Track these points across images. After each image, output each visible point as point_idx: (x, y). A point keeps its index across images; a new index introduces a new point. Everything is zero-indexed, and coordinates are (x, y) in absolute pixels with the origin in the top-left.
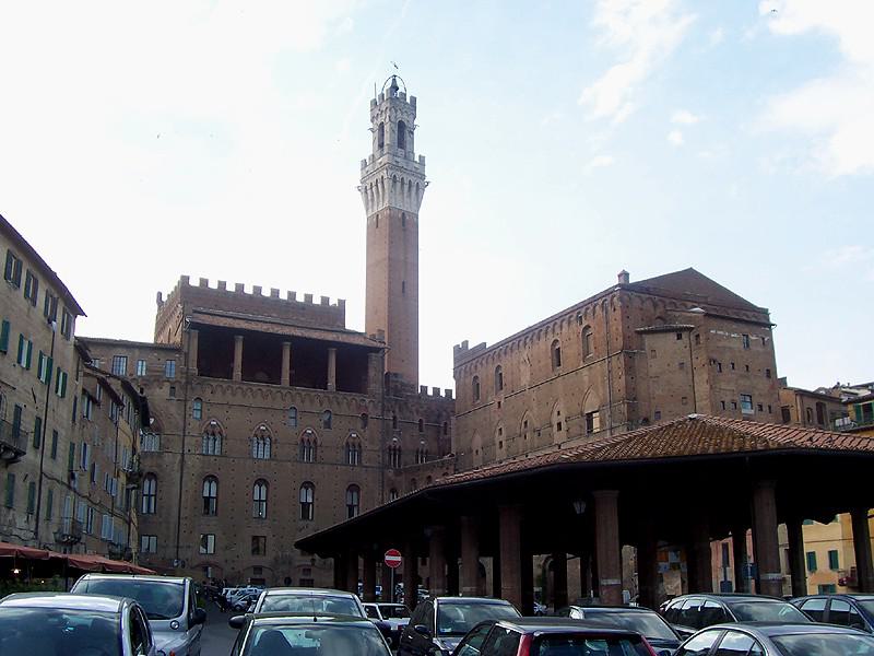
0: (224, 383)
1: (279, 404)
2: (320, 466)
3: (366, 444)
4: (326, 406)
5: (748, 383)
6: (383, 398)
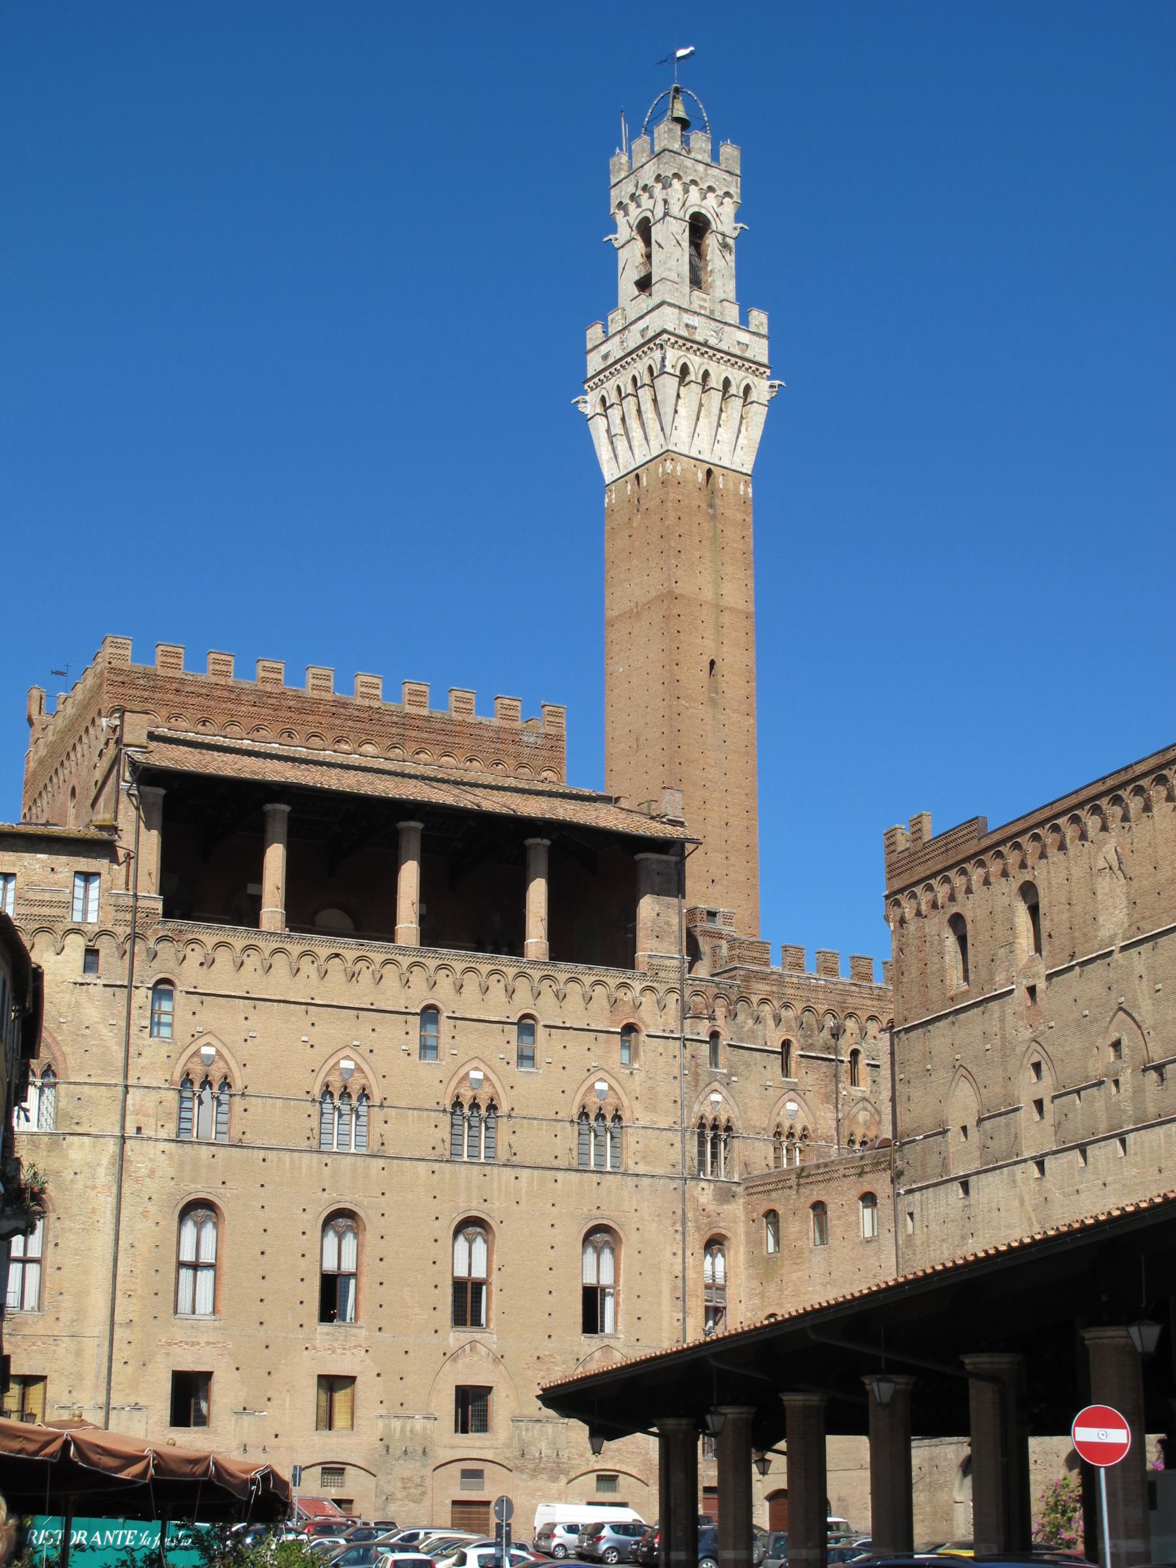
0: (238, 937)
1: (391, 994)
2: (509, 1173)
3: (634, 1112)
4: (523, 1003)
6: (682, 980)
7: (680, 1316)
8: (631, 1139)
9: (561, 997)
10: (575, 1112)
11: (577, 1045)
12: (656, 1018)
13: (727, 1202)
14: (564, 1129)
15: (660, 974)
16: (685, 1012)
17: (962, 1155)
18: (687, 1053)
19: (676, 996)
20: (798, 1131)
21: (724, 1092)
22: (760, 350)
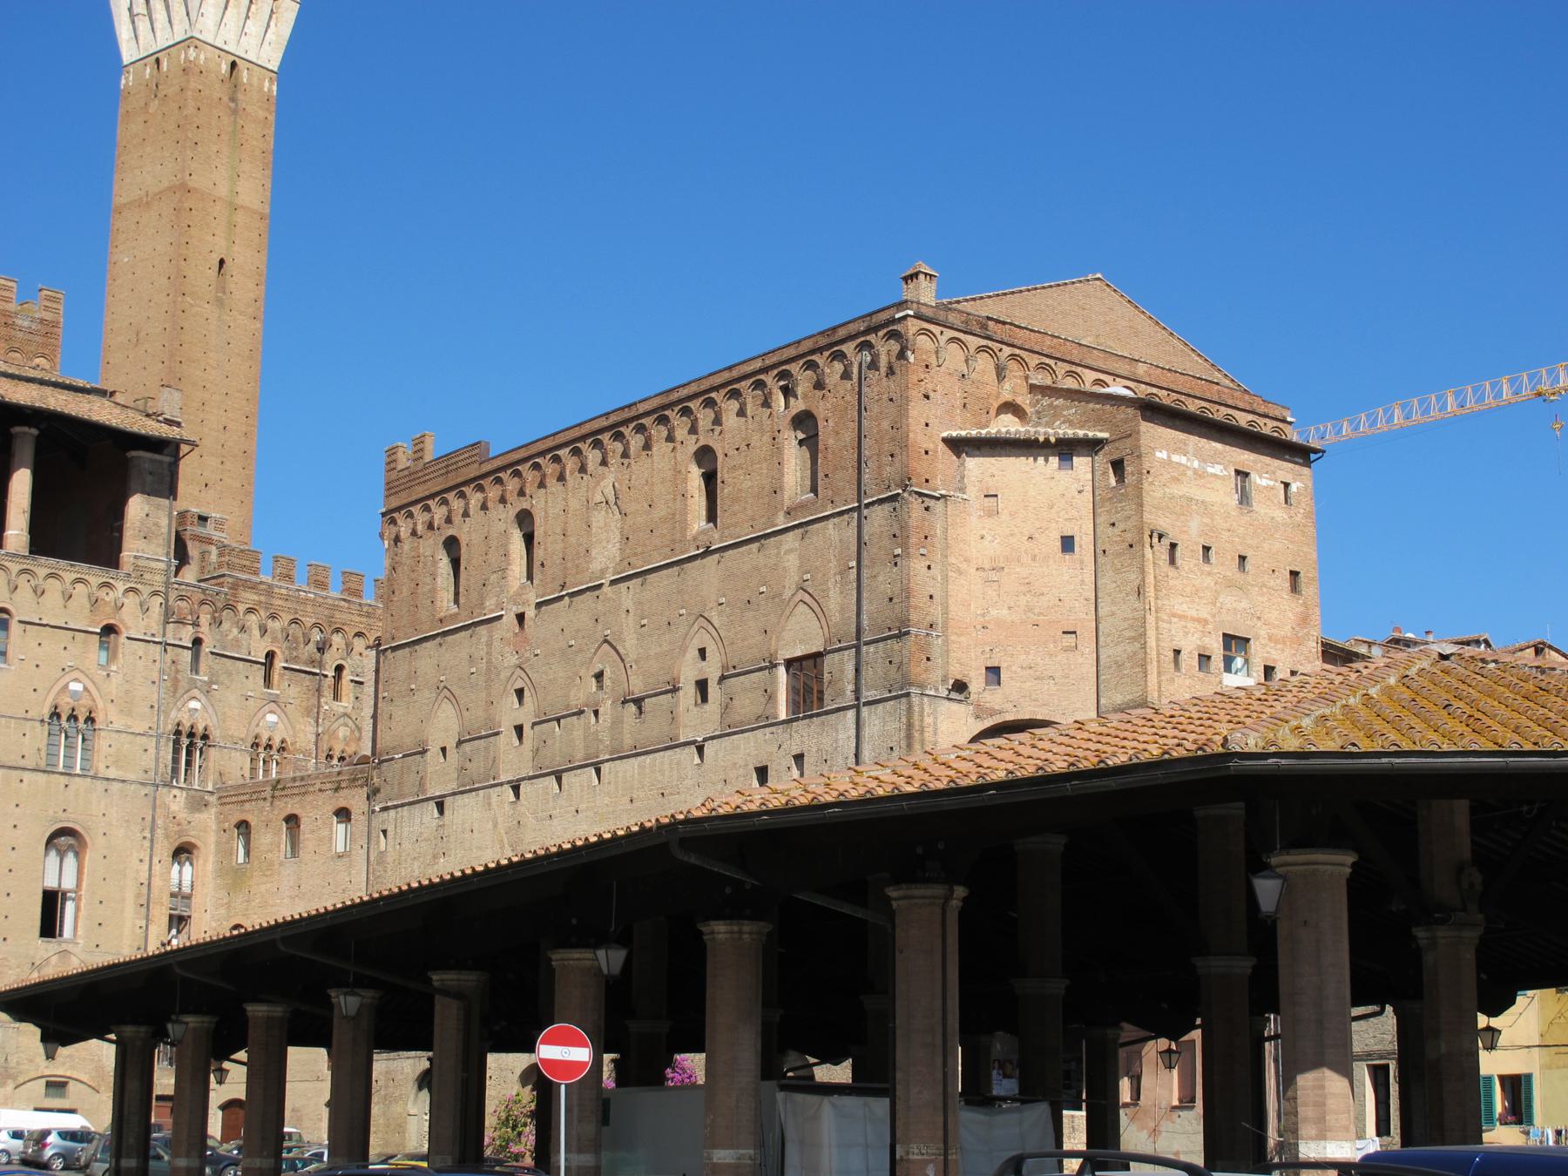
3: (108, 715)
5: (1244, 604)
6: (167, 584)
7: (143, 923)
8: (102, 743)
9: (39, 593)
10: (46, 712)
11: (53, 643)
12: (138, 620)
13: (199, 811)
14: (33, 728)
15: (147, 576)
16: (168, 616)
17: (439, 775)
18: (168, 658)
19: (160, 600)
20: (276, 743)
21: (204, 700)
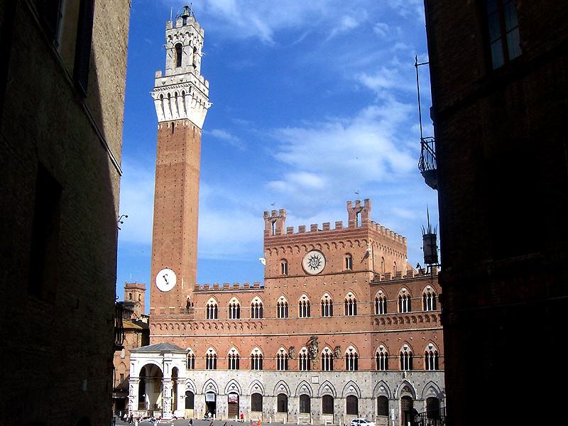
22: (207, 92)
